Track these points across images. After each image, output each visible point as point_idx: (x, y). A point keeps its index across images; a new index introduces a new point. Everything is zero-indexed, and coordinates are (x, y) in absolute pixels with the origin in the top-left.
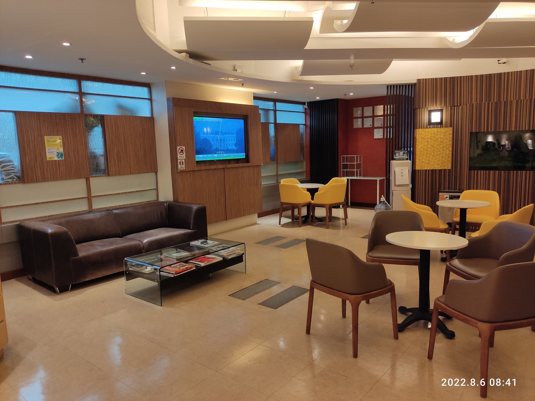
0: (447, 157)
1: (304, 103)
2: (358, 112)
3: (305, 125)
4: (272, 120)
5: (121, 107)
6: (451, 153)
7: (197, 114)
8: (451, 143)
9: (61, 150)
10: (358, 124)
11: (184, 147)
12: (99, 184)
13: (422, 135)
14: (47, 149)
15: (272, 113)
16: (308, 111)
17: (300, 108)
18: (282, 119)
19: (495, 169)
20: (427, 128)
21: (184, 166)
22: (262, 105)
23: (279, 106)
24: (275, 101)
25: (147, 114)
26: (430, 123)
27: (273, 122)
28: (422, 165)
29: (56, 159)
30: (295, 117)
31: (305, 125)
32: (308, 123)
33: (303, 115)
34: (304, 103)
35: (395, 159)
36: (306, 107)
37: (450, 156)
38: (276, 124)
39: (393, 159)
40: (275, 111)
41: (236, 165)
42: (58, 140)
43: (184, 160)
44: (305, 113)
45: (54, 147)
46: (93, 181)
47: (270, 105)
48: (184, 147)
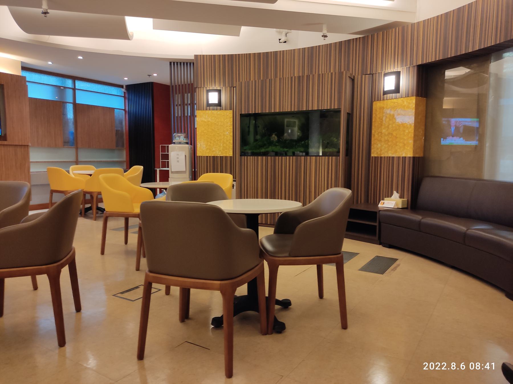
0: (228, 143)
1: (122, 87)
2: (177, 99)
3: (125, 110)
4: (70, 99)
6: (232, 138)
8: (232, 127)
10: (177, 111)
13: (202, 118)
15: (70, 93)
16: (127, 96)
17: (120, 92)
18: (82, 99)
19: (265, 154)
20: (207, 110)
22: (30, 76)
23: (79, 85)
24: (74, 78)
26: (209, 105)
27: (72, 101)
28: (203, 150)
30: (115, 101)
31: (125, 110)
32: (127, 109)
33: (123, 99)
34: (122, 87)
35: (174, 143)
36: (123, 90)
37: (232, 141)
38: (75, 105)
39: (171, 142)
44: (125, 97)
47: (69, 83)
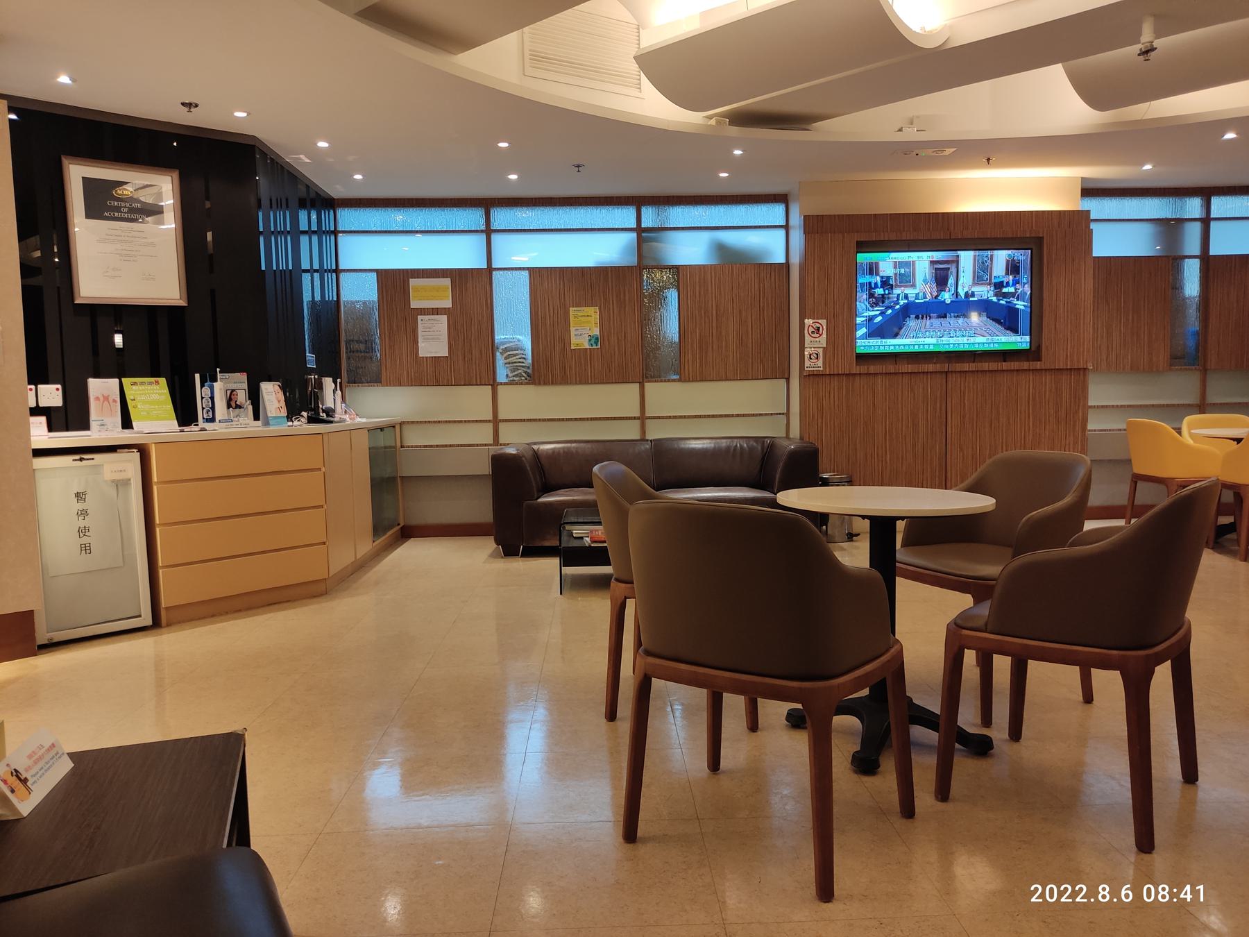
5: (722, 249)
7: (863, 247)
9: (596, 331)
11: (824, 322)
12: (667, 396)
14: (572, 329)
18: (1225, 243)
21: (820, 363)
22: (1098, 208)
23: (1220, 206)
25: (782, 260)
27: (1197, 252)
29: (587, 346)
38: (1206, 259)
40: (1206, 221)
41: (994, 366)
42: (592, 313)
43: (821, 351)
45: (584, 327)
46: (649, 386)
47: (1193, 207)
48: (824, 322)
